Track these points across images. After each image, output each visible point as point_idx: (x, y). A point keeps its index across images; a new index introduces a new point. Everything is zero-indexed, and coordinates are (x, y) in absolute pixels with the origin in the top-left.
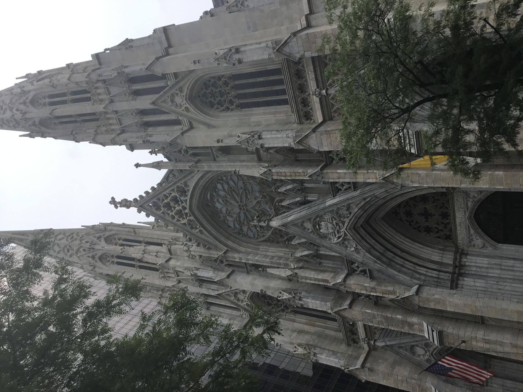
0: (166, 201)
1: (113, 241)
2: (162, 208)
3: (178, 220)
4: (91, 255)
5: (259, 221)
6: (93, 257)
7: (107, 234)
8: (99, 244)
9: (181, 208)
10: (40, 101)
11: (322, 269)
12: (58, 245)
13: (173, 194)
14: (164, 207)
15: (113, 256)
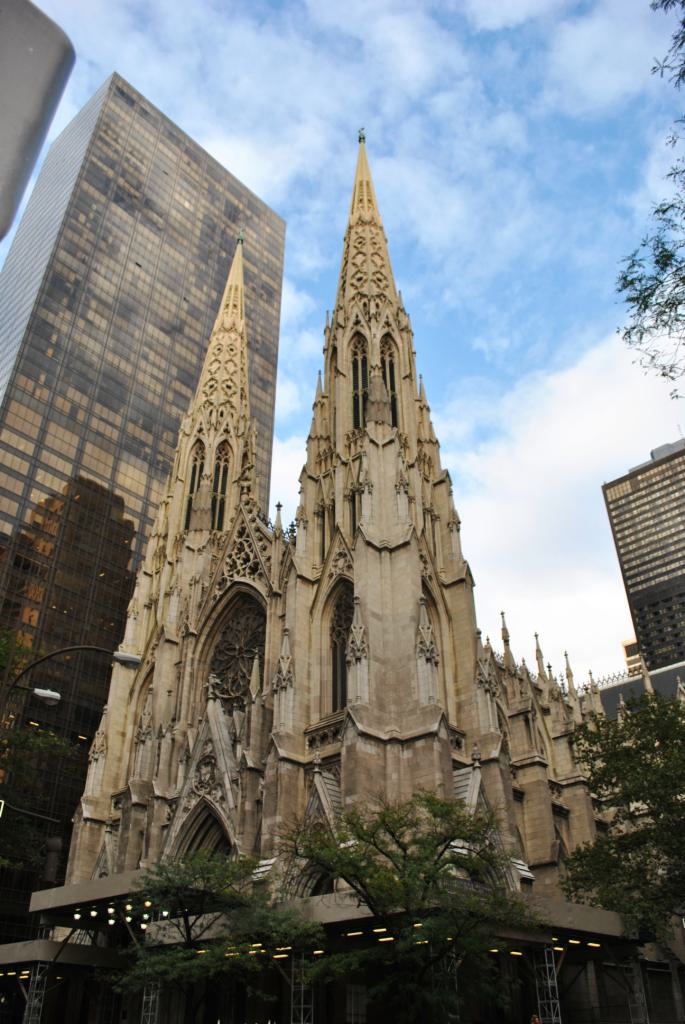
0: (246, 545)
1: (223, 453)
2: (240, 540)
3: (227, 563)
4: (204, 426)
5: (213, 687)
6: (200, 431)
7: (233, 442)
8: (215, 436)
9: (239, 568)
10: (359, 346)
11: (174, 764)
12: (219, 368)
13: (252, 556)
14: (241, 544)
15: (203, 458)
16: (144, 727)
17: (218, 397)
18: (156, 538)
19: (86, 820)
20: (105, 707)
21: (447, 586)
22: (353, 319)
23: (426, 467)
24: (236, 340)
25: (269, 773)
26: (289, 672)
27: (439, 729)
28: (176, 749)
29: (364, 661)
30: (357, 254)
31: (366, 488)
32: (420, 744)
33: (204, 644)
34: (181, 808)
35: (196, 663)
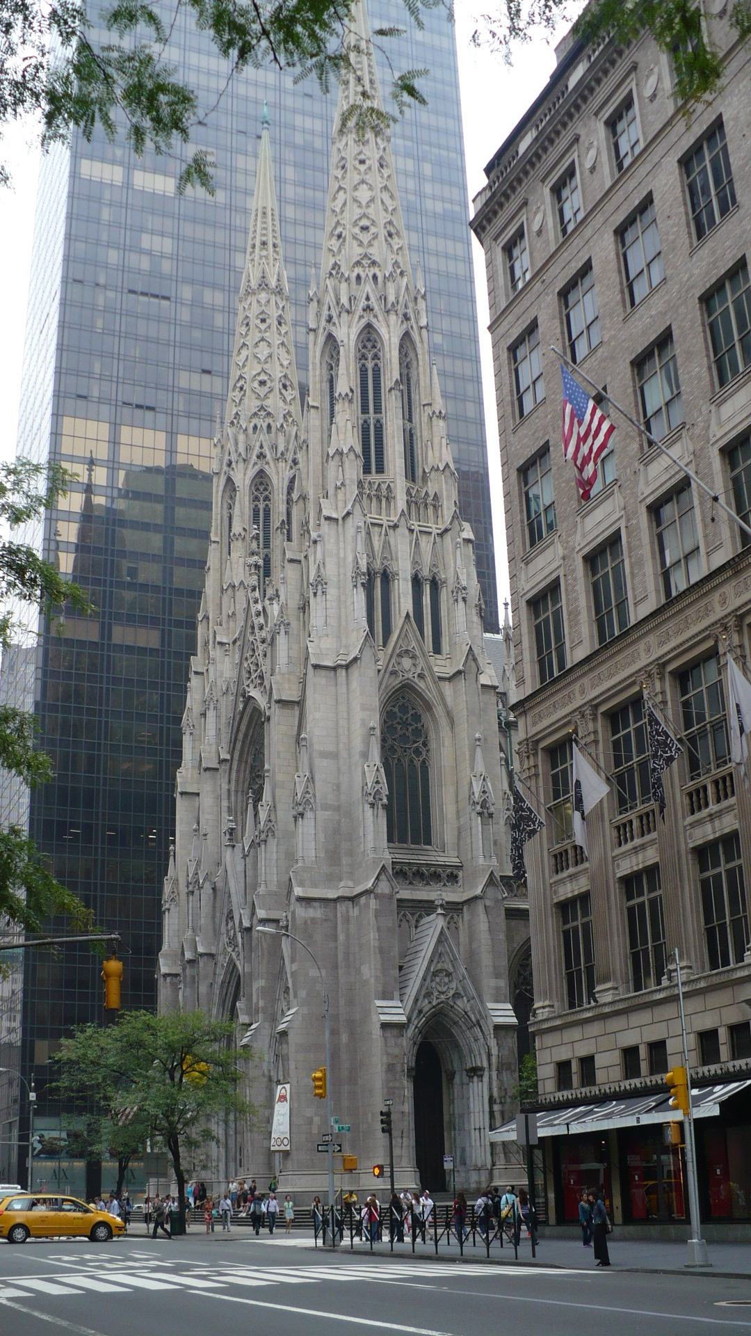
1: (261, 488)
4: (234, 457)
7: (270, 470)
9: (253, 677)
16: (190, 875)
17: (251, 404)
18: (204, 621)
19: (165, 976)
20: (171, 848)
21: (450, 679)
22: (325, 313)
23: (430, 510)
24: (268, 301)
25: (255, 934)
26: (270, 821)
27: (375, 885)
28: (218, 898)
29: (309, 814)
30: (338, 191)
31: (320, 587)
32: (363, 900)
33: (238, 771)
34: (219, 965)
35: (233, 793)
